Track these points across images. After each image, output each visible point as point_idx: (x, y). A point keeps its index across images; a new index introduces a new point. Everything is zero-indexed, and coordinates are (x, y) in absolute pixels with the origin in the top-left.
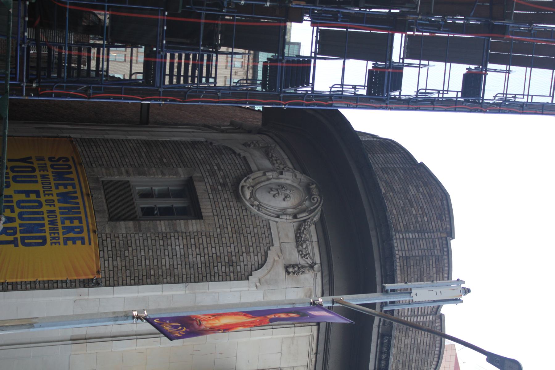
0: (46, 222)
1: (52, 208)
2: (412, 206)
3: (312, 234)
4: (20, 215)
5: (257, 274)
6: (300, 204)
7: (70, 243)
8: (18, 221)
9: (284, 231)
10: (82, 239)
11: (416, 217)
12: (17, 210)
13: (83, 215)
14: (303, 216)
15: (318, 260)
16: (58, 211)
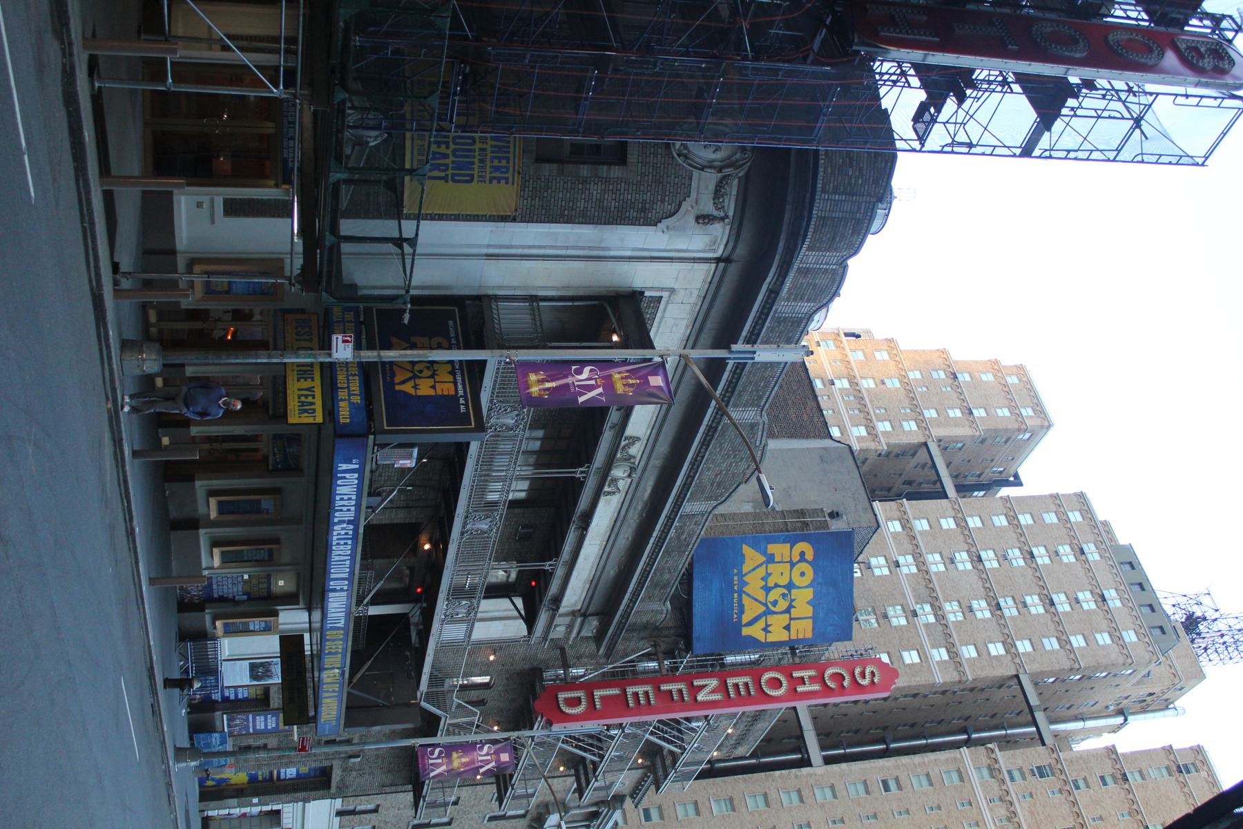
0: (476, 160)
1: (484, 146)
2: (851, 166)
3: (733, 188)
4: (454, 151)
5: (665, 222)
6: (729, 157)
7: (495, 182)
8: (451, 158)
9: (704, 183)
10: (507, 180)
11: (850, 178)
12: (452, 146)
13: (511, 156)
14: (728, 171)
15: (731, 214)
16: (489, 149)
